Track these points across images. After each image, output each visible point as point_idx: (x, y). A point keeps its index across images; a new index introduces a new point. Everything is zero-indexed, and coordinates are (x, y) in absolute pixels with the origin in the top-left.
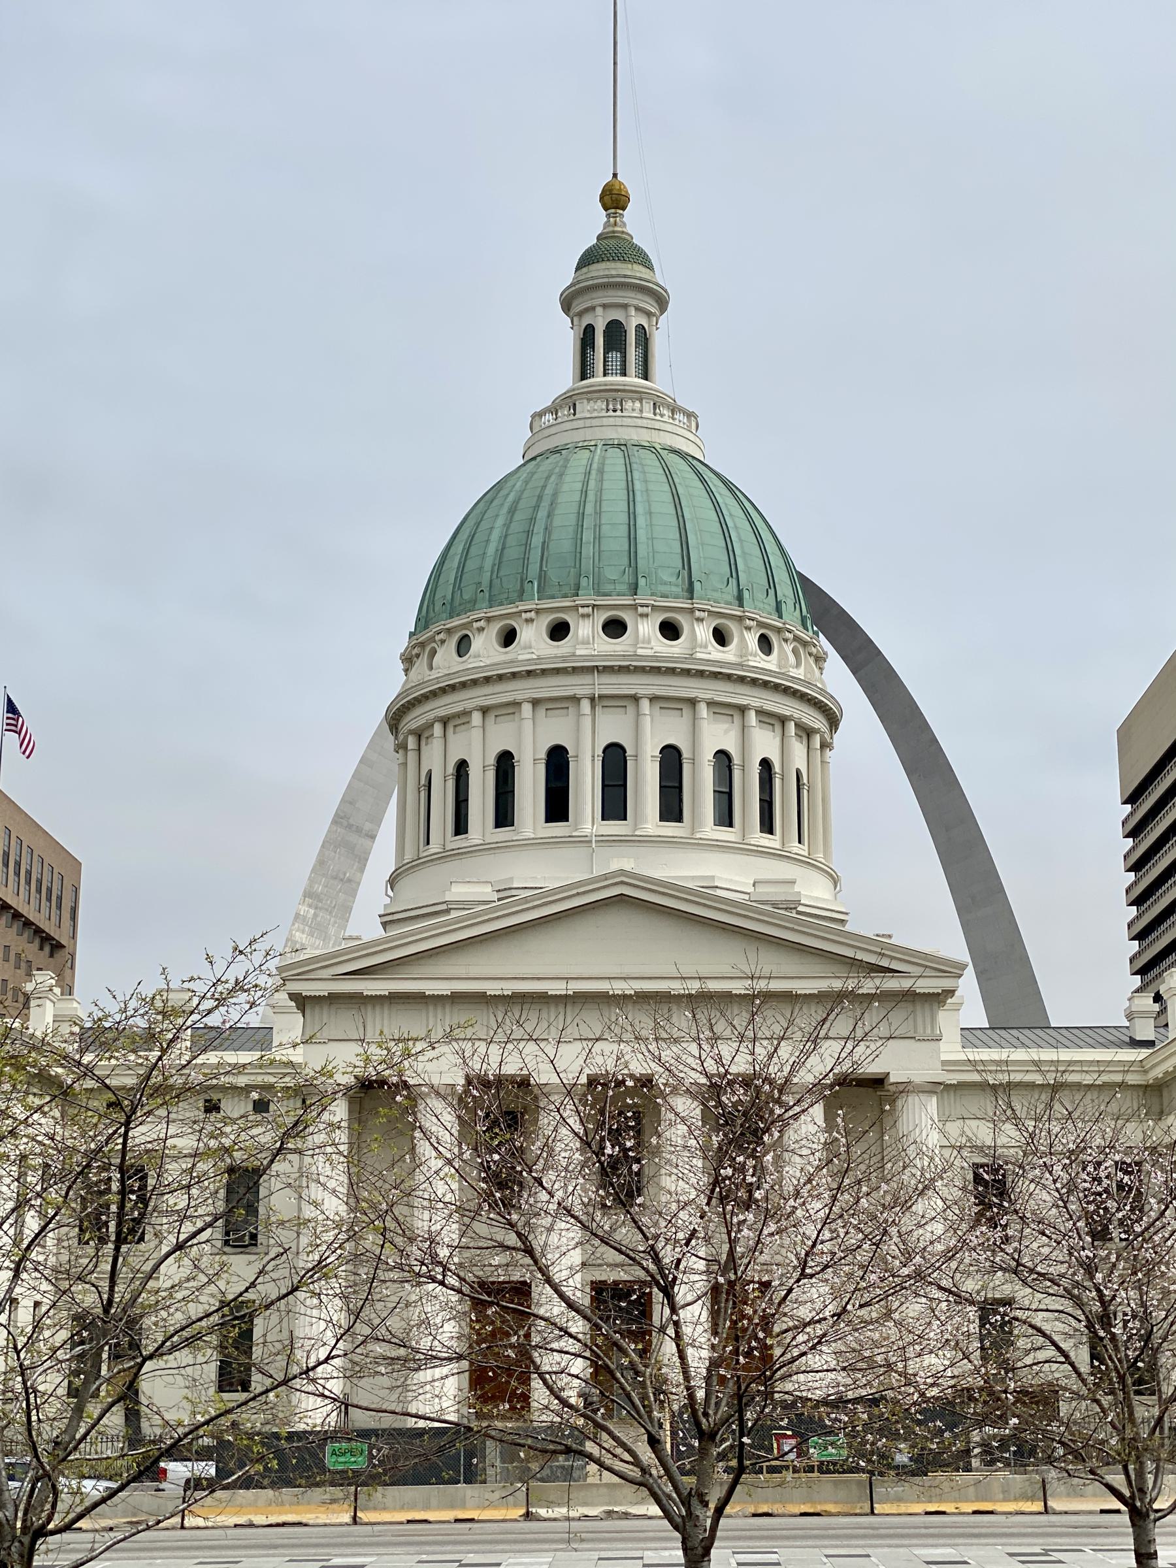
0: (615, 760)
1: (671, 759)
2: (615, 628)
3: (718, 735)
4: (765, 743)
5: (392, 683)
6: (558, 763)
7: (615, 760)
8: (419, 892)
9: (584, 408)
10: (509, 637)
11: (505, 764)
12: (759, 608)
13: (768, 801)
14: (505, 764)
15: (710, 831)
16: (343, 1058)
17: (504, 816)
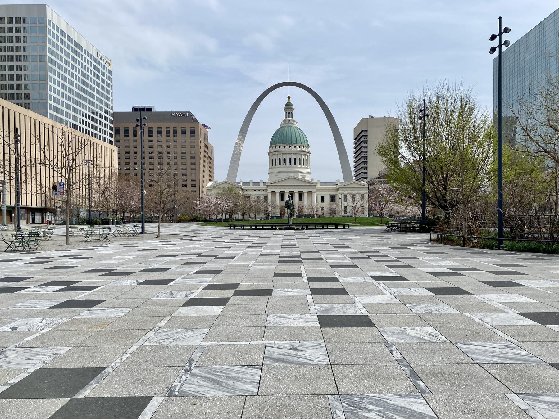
0: (290, 159)
1: (295, 159)
2: (290, 147)
3: (299, 157)
4: (303, 157)
5: (268, 150)
6: (285, 159)
7: (290, 159)
8: (272, 171)
9: (287, 122)
10: (280, 147)
11: (280, 159)
12: (303, 144)
13: (304, 163)
14: (280, 159)
15: (299, 166)
16: (270, 190)
17: (280, 164)
